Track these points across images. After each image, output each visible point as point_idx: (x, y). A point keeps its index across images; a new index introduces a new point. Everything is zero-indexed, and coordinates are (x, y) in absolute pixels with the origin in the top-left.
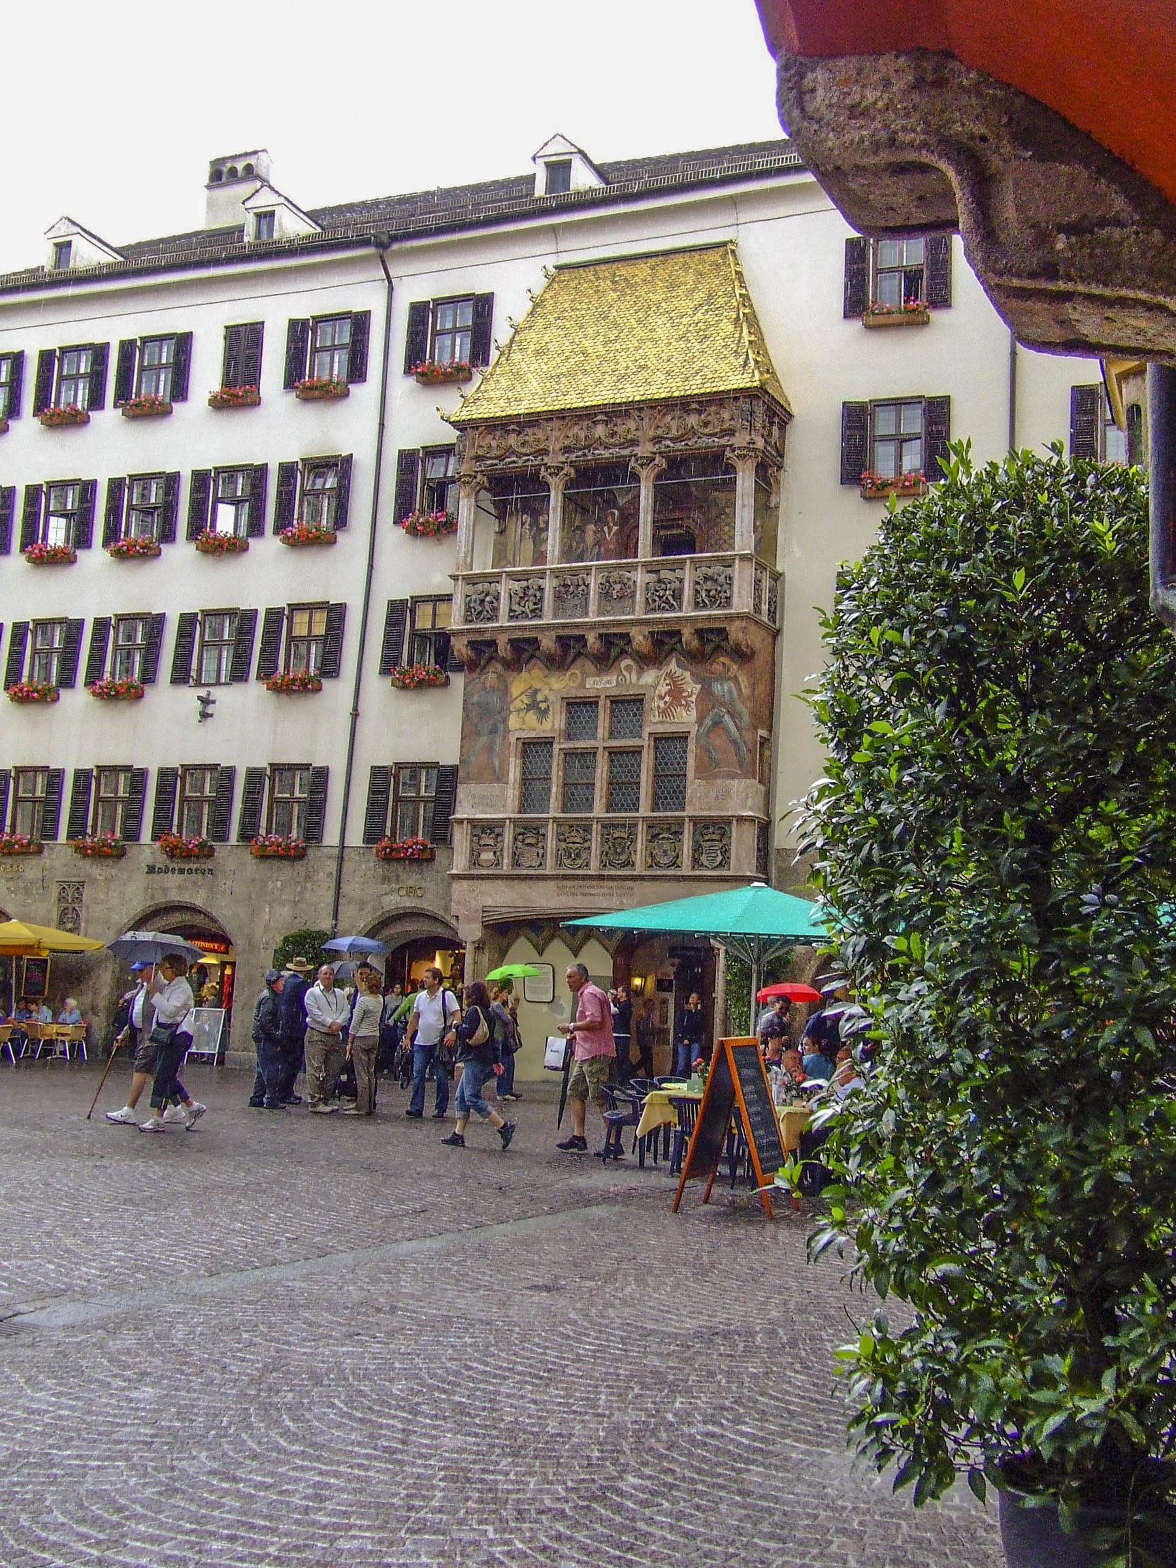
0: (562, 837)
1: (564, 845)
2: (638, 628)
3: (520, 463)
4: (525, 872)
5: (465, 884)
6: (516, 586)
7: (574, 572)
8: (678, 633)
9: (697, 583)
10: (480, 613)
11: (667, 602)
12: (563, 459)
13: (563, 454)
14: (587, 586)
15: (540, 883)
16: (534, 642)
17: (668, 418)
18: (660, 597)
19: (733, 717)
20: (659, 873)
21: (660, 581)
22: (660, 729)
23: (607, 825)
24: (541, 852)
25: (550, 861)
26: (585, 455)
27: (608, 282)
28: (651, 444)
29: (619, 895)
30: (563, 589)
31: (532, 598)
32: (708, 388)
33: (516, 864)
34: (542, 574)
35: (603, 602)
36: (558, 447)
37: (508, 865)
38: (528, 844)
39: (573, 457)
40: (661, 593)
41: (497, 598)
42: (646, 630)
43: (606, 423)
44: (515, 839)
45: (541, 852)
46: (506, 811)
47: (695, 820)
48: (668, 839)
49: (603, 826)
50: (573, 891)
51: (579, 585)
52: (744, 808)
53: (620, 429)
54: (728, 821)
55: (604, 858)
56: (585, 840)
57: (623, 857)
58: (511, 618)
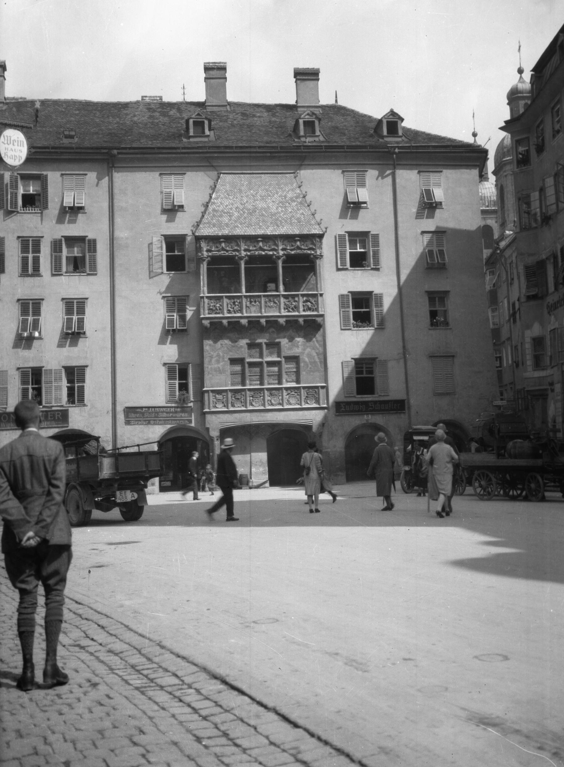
6: (228, 301)
12: (245, 253)
22: (286, 355)
38: (237, 399)
39: (249, 254)
41: (222, 305)
42: (284, 319)
44: (231, 397)
54: (317, 387)
55: (269, 402)
58: (228, 313)
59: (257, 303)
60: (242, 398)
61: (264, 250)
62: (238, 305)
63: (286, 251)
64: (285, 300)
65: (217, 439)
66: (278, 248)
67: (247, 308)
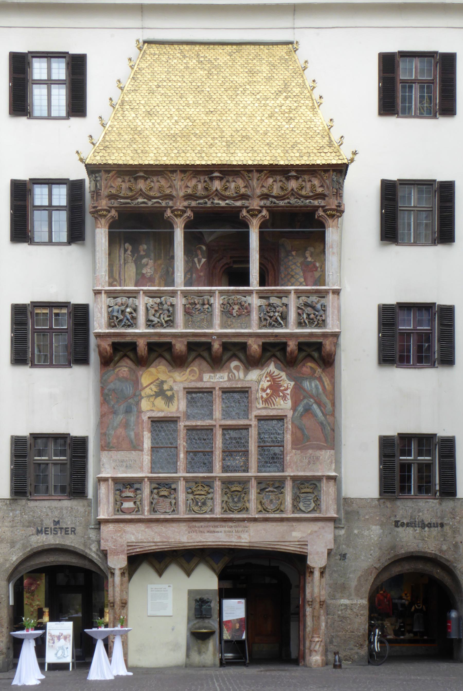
0: (190, 491)
1: (191, 496)
2: (253, 339)
3: (150, 204)
4: (162, 516)
5: (111, 527)
6: (151, 301)
7: (200, 294)
8: (285, 345)
9: (299, 308)
10: (121, 321)
11: (276, 321)
12: (186, 203)
13: (186, 200)
14: (211, 305)
15: (174, 525)
16: (168, 346)
17: (270, 180)
18: (271, 317)
19: (319, 404)
20: (268, 516)
21: (269, 305)
23: (227, 483)
24: (173, 501)
25: (182, 506)
26: (206, 203)
27: (195, 61)
28: (258, 199)
29: (237, 532)
30: (190, 306)
31: (166, 312)
32: (305, 161)
33: (153, 510)
34: (173, 294)
35: (225, 318)
36: (181, 194)
37: (148, 512)
39: (194, 204)
40: (272, 314)
41: (135, 310)
42: (260, 342)
43: (221, 179)
44: (152, 492)
45: (173, 501)
46: (142, 471)
47: (294, 479)
48: (272, 492)
49: (223, 483)
50: (201, 529)
51: (203, 304)
52: (329, 470)
53: (233, 185)
55: (224, 505)
56: (209, 493)
57: (240, 505)
58: (148, 326)
59: (207, 306)
60: (173, 496)
61: (224, 198)
62: (168, 311)
63: (267, 199)
64: (263, 302)
65: (123, 574)
66: (253, 195)
67: (188, 316)
